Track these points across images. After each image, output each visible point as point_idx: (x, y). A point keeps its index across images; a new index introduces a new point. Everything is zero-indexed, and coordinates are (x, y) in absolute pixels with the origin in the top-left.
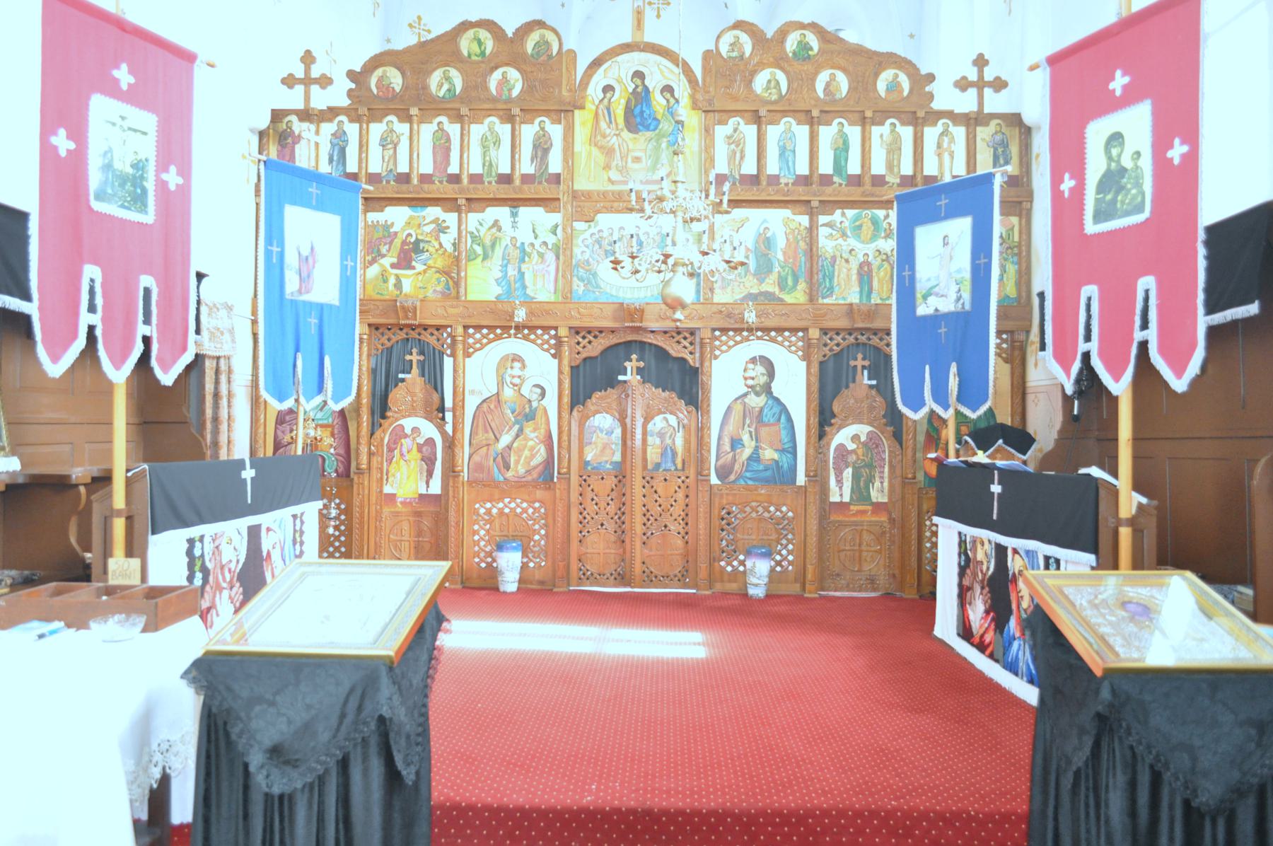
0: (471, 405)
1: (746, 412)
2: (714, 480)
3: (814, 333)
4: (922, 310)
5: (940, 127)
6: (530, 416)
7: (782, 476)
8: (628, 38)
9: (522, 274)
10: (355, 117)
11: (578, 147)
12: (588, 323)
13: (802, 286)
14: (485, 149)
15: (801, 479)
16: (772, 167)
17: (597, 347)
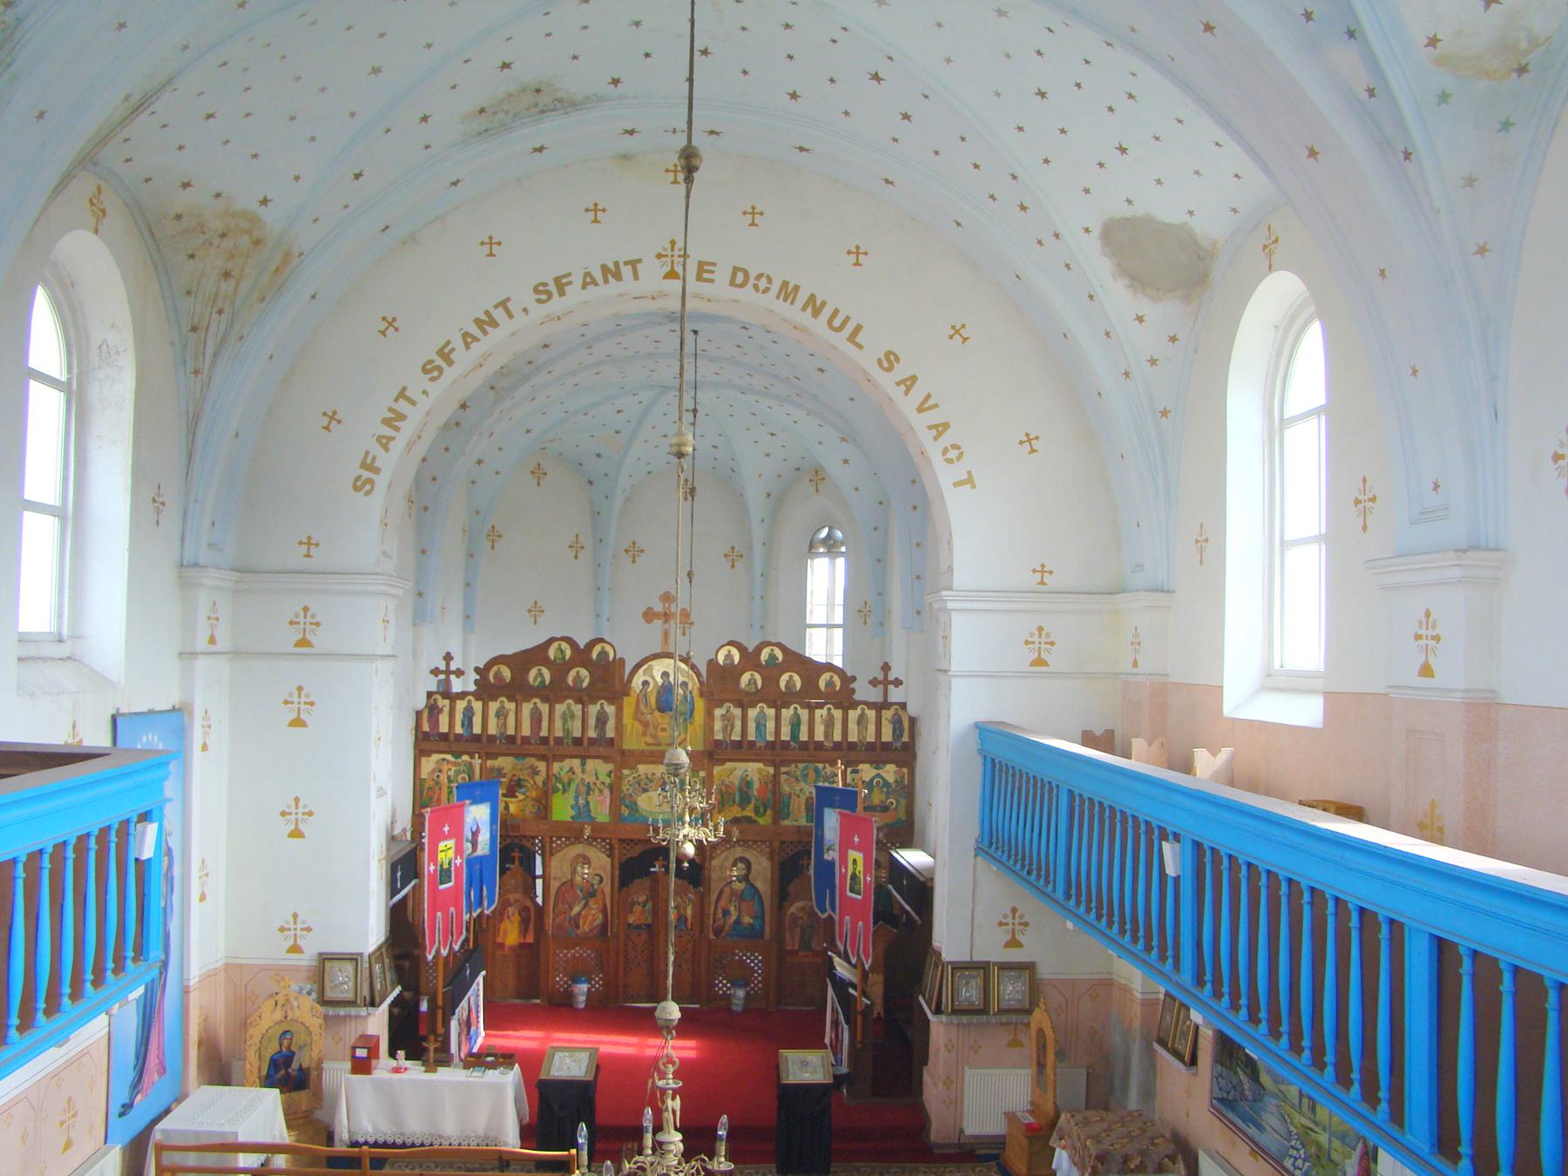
0: (555, 885)
1: (733, 893)
2: (712, 937)
3: (776, 844)
4: (826, 857)
5: (859, 711)
7: (754, 934)
9: (588, 803)
10: (478, 695)
11: (625, 720)
13: (769, 812)
14: (565, 721)
15: (767, 936)
16: (751, 737)
17: (637, 850)
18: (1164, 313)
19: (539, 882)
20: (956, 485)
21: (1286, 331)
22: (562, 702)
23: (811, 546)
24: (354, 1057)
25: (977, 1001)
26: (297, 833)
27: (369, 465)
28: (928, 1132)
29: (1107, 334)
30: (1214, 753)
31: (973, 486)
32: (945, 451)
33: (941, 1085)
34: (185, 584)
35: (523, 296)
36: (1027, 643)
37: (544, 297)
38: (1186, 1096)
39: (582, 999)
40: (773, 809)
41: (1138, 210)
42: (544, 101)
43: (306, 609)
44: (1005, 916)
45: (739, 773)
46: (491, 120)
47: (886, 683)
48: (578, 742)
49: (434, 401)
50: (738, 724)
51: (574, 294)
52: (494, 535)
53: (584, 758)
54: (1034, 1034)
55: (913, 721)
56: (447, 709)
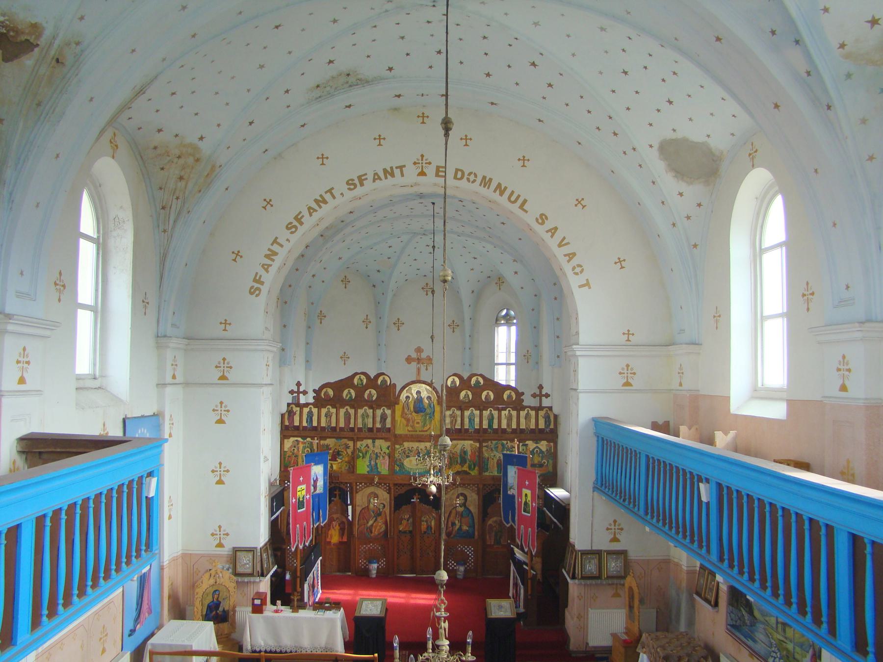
0: (358, 509)
1: (457, 513)
3: (481, 486)
5: (526, 411)
6: (380, 514)
7: (469, 536)
8: (414, 379)
10: (315, 405)
12: (400, 482)
13: (477, 468)
16: (466, 427)
17: (403, 491)
18: (694, 191)
19: (350, 508)
20: (580, 286)
21: (762, 201)
22: (361, 408)
23: (497, 320)
24: (253, 604)
25: (595, 572)
26: (220, 482)
27: (258, 280)
28: (569, 646)
29: (663, 203)
30: (726, 433)
31: (590, 288)
32: (574, 268)
33: (575, 619)
34: (159, 347)
35: (341, 187)
36: (620, 373)
37: (352, 187)
38: (712, 624)
39: (374, 572)
40: (479, 467)
41: (679, 135)
42: (351, 80)
43: (224, 359)
44: (610, 525)
45: (459, 447)
46: (323, 91)
47: (541, 396)
48: (371, 430)
49: (292, 245)
50: (459, 419)
51: (369, 184)
52: (322, 316)
53: (374, 439)
54: (627, 590)
55: (556, 417)
56: (298, 413)
